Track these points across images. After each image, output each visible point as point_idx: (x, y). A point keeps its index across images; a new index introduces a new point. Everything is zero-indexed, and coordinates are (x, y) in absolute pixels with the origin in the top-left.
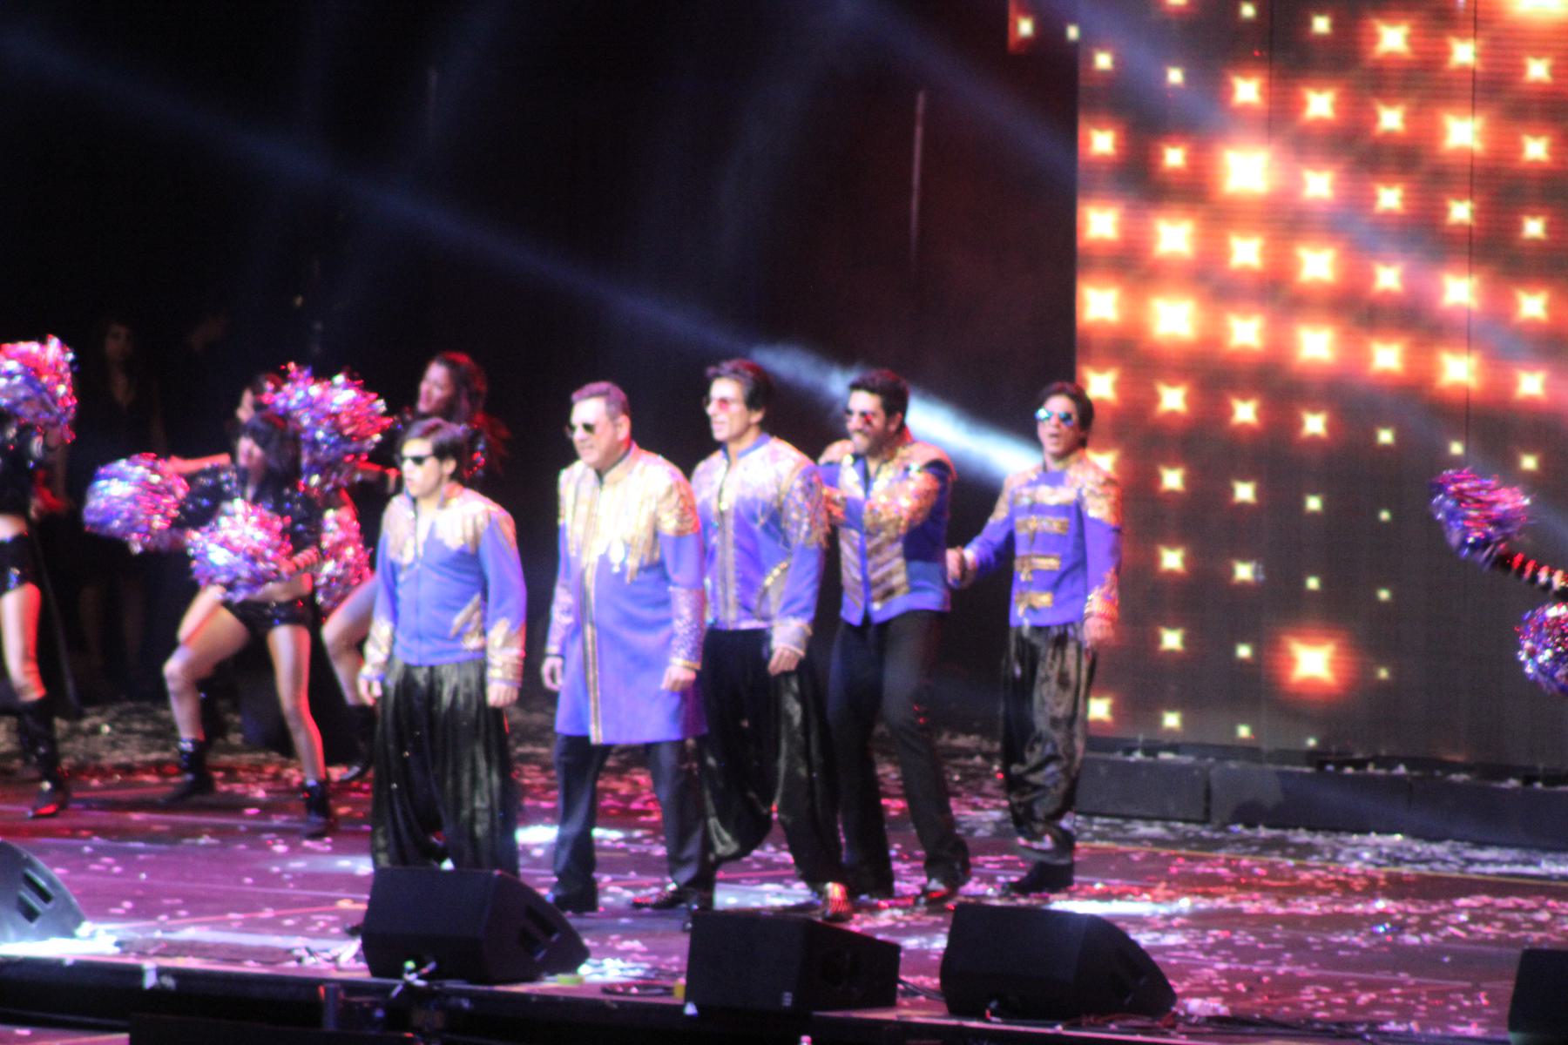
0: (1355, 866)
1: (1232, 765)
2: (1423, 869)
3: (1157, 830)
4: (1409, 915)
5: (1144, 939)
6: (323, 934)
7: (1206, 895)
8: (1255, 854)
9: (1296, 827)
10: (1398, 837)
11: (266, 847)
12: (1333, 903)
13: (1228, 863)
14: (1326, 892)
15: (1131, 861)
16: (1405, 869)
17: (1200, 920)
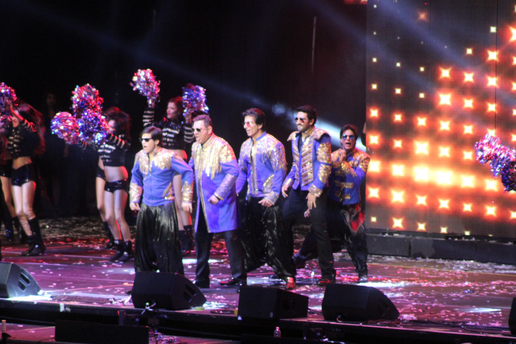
0: (458, 271)
1: (418, 238)
2: (481, 271)
3: (393, 259)
4: (476, 287)
5: (389, 295)
6: (119, 294)
7: (409, 280)
8: (425, 267)
9: (439, 258)
10: (472, 261)
11: (100, 265)
12: (451, 283)
13: (416, 270)
14: (449, 279)
15: (384, 269)
16: (475, 272)
17: (407, 289)
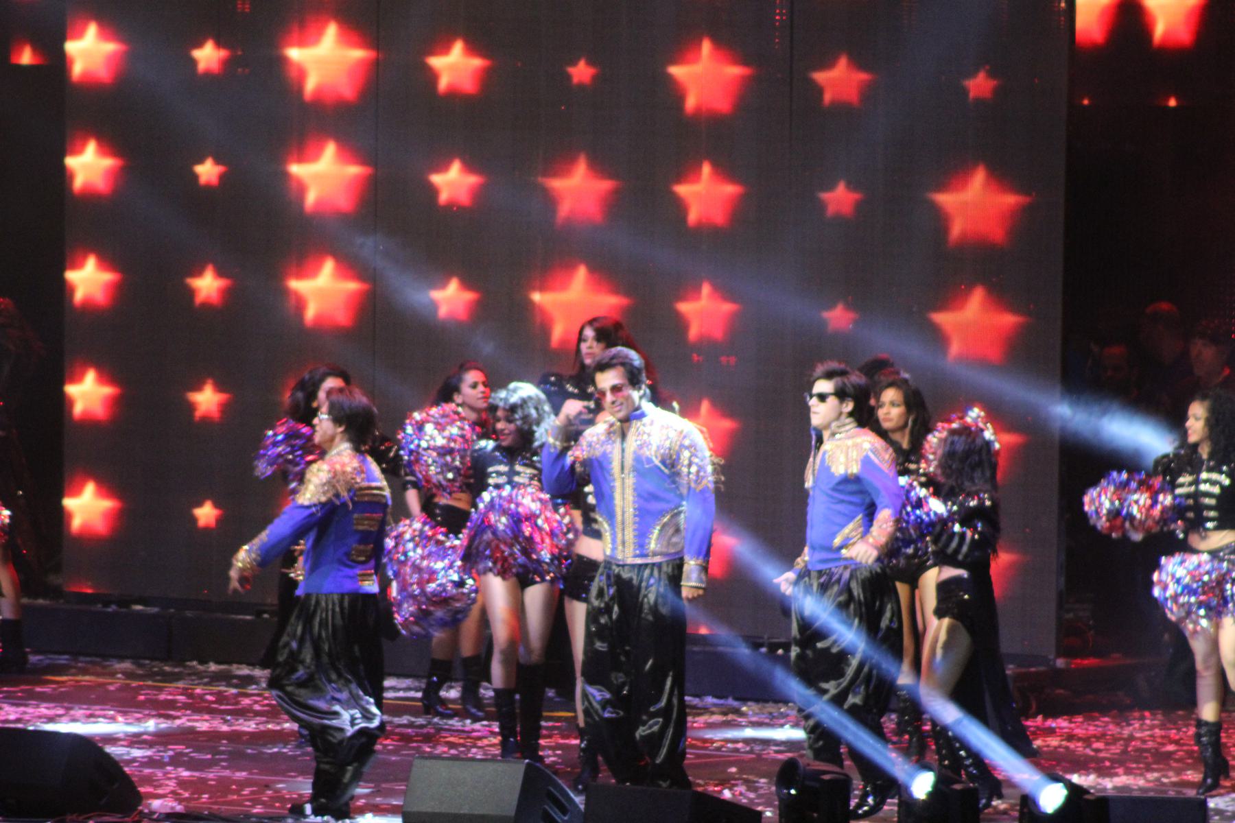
1: (189, 614)
7: (168, 717)
8: (205, 684)
9: (240, 663)
13: (185, 692)
14: (257, 714)
15: (108, 691)
17: (161, 739)
